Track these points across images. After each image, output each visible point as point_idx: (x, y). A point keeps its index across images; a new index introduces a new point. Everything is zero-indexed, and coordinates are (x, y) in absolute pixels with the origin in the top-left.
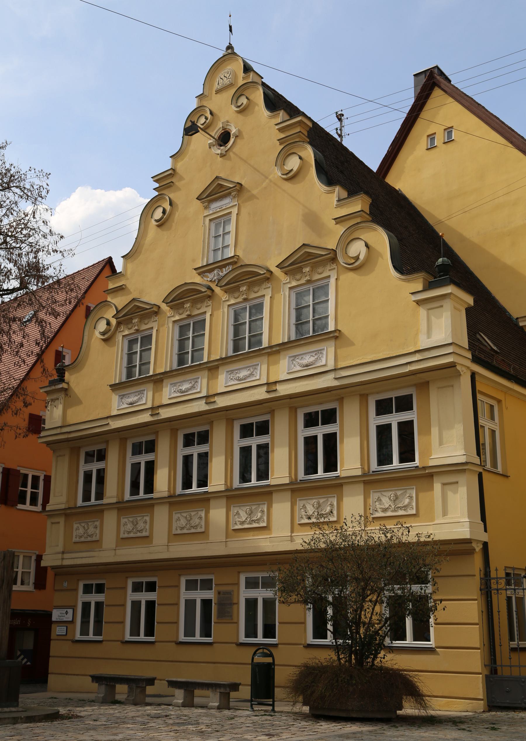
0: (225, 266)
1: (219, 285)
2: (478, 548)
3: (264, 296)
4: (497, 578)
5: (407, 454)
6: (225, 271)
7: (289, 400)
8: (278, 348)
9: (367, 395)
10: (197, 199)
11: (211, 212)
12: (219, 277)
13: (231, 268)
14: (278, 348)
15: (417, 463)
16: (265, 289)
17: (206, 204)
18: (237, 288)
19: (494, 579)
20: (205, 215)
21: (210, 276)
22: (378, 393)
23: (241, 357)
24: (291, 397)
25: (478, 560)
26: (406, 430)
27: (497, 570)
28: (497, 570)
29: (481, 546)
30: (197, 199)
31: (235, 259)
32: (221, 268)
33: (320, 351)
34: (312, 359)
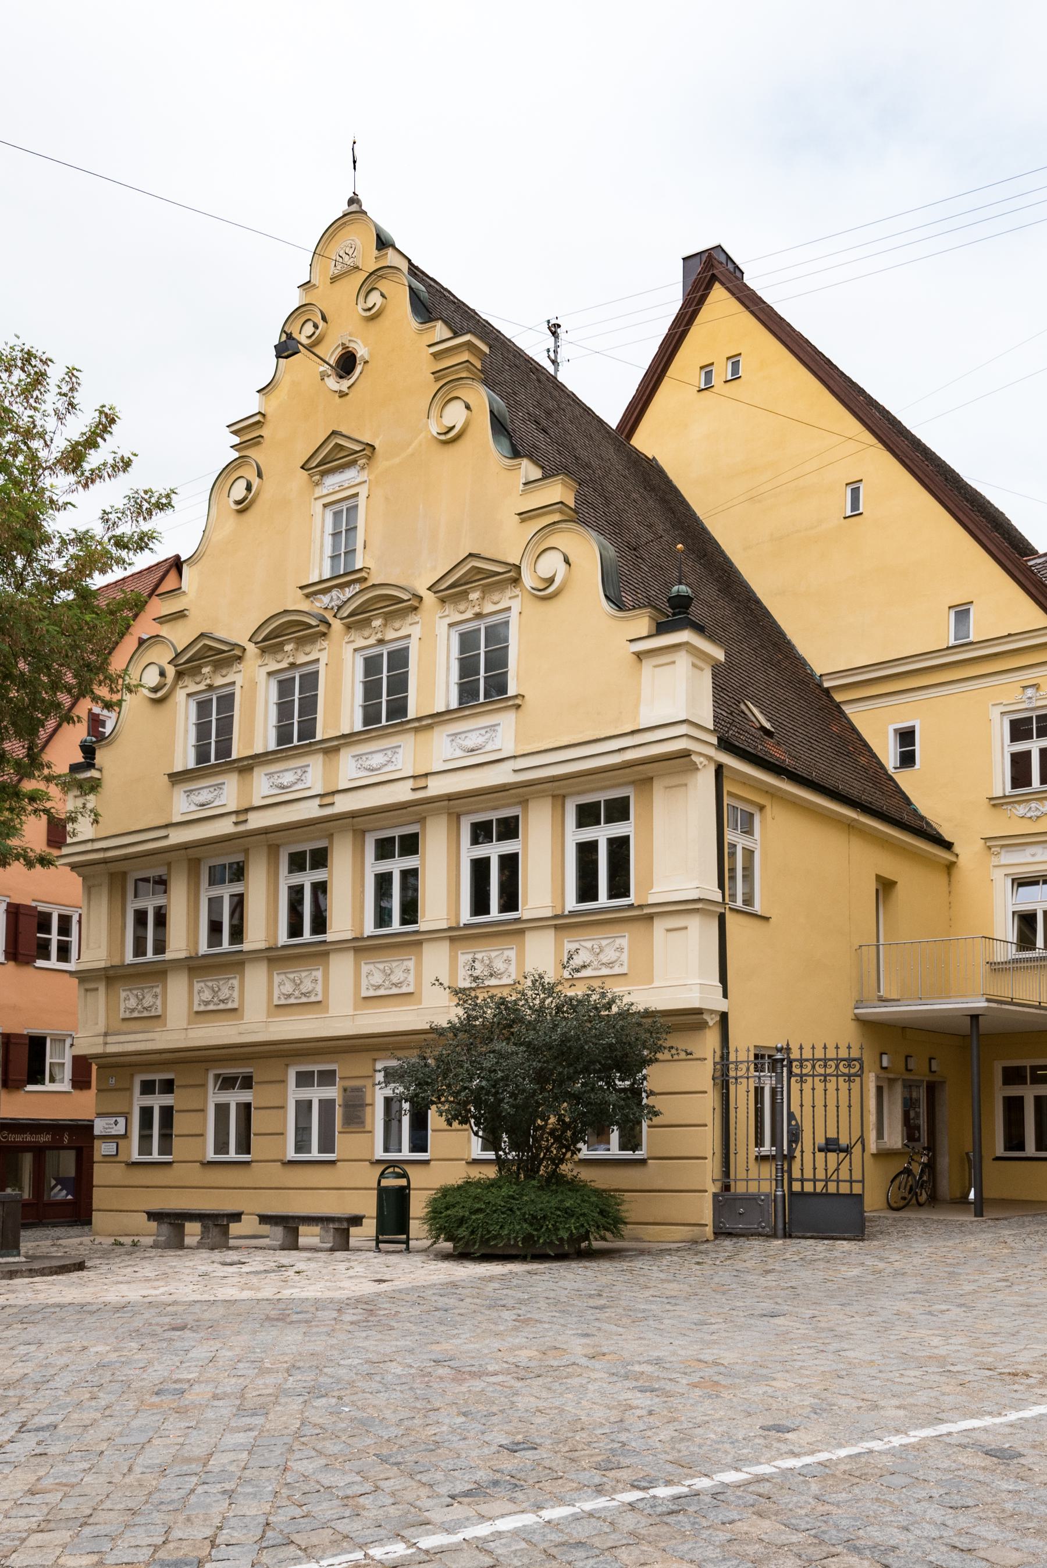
0: (348, 584)
1: (338, 616)
2: (712, 1020)
3: (409, 636)
4: (736, 1062)
5: (619, 887)
6: (348, 592)
7: (446, 802)
8: (429, 721)
9: (564, 797)
10: (302, 467)
11: (325, 492)
12: (339, 603)
13: (358, 587)
14: (429, 721)
15: (632, 899)
16: (411, 625)
17: (318, 477)
18: (367, 622)
19: (732, 1063)
20: (316, 496)
21: (325, 599)
22: (579, 793)
23: (374, 734)
24: (450, 798)
25: (709, 1043)
26: (619, 847)
27: (737, 1051)
28: (737, 1051)
29: (718, 1018)
30: (302, 467)
31: (364, 574)
32: (341, 586)
33: (493, 727)
34: (480, 740)
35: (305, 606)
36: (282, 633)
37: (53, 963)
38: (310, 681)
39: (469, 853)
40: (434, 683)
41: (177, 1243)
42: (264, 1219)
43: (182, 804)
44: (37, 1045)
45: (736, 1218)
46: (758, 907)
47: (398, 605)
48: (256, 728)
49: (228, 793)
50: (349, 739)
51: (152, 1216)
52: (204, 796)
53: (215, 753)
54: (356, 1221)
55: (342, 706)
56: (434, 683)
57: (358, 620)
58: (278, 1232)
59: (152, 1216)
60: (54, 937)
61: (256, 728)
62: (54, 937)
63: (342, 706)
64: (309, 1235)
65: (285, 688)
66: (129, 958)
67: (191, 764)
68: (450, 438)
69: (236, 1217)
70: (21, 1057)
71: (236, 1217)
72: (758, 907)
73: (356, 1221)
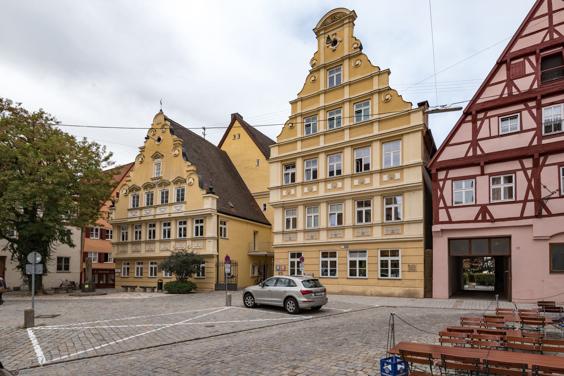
6: (159, 180)
18: (161, 186)
35: (151, 182)
36: (147, 186)
37: (109, 239)
38: (152, 195)
39: (178, 226)
40: (173, 198)
41: (127, 291)
42: (140, 287)
43: (130, 215)
44: (106, 255)
45: (219, 287)
46: (227, 237)
47: (168, 184)
48: (143, 202)
49: (138, 213)
50: (158, 206)
51: (122, 286)
52: (134, 213)
53: (136, 206)
54: (155, 287)
55: (158, 200)
56: (173, 198)
57: (160, 185)
58: (142, 289)
59: (122, 286)
60: (110, 234)
61: (143, 202)
62: (110, 234)
63: (158, 200)
64: (148, 290)
65: (148, 195)
66: (121, 241)
67: (132, 207)
68: (176, 156)
69: (136, 287)
70: (103, 257)
71: (136, 287)
72: (227, 237)
73: (155, 287)
